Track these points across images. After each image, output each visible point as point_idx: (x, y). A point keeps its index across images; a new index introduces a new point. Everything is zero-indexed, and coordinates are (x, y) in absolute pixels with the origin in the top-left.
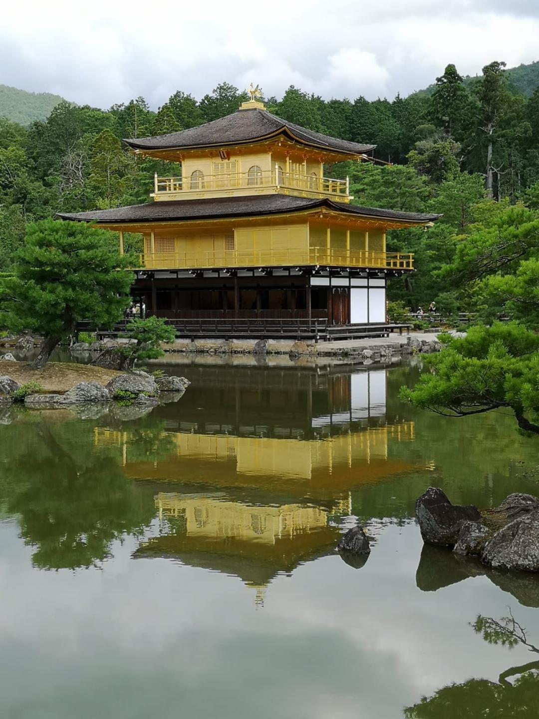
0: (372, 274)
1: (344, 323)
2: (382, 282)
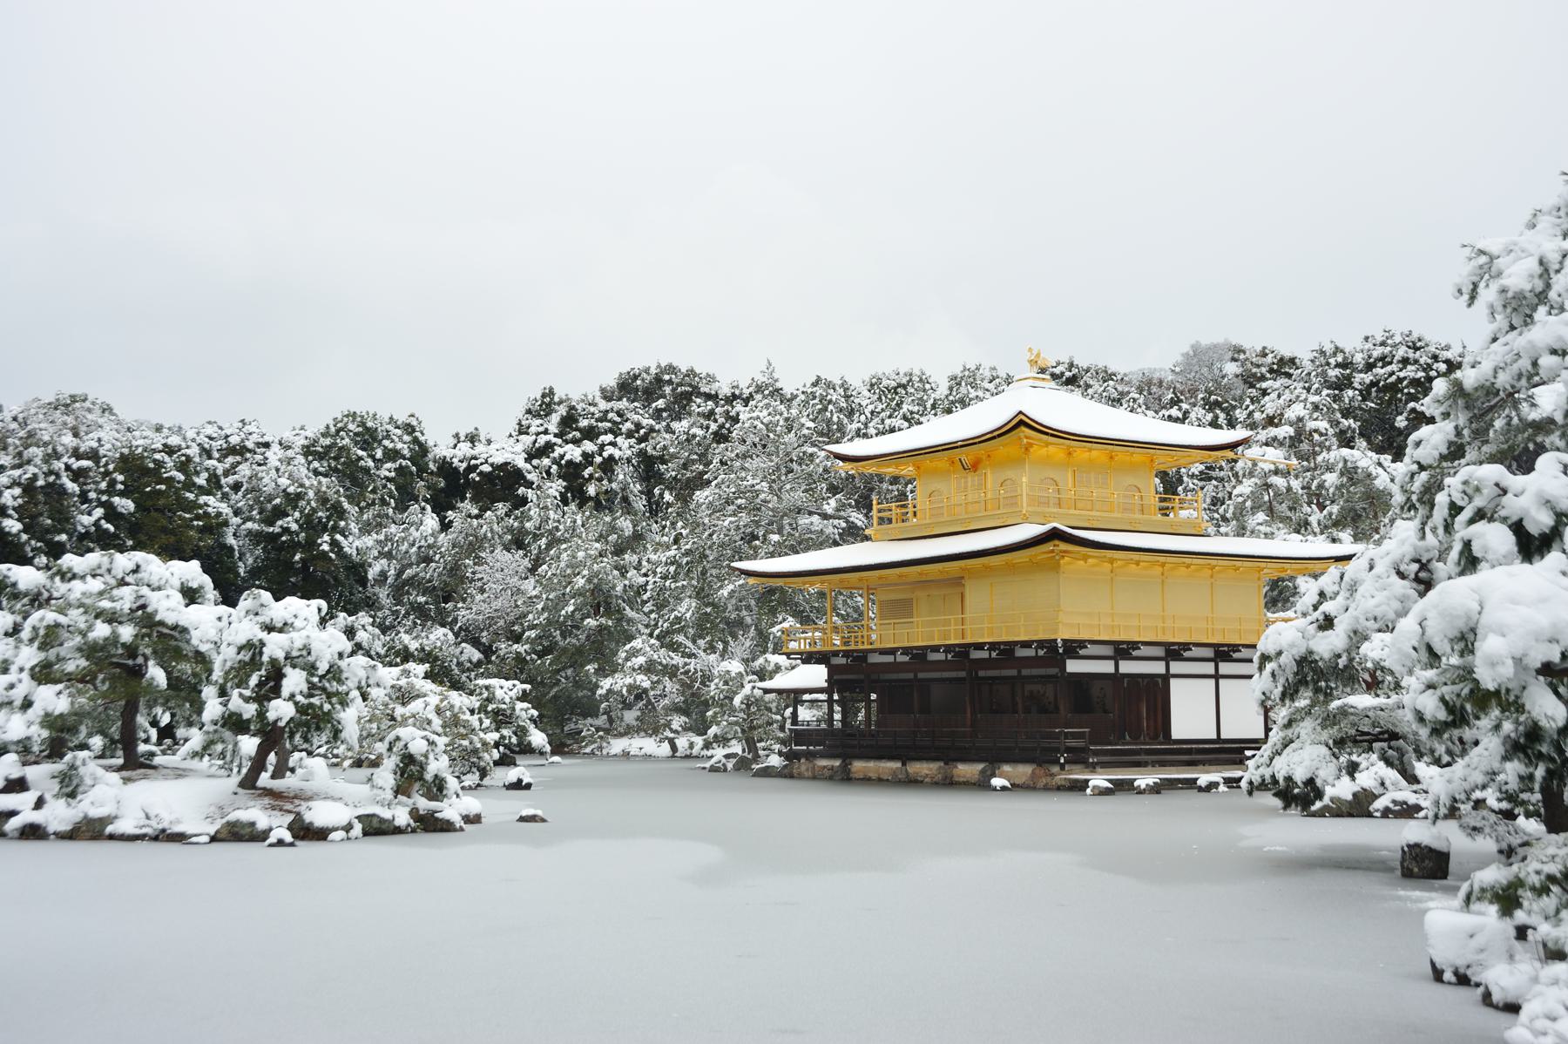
1: (1154, 739)
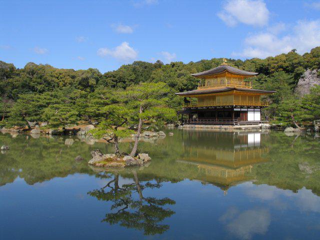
0: (255, 108)
2: (259, 110)
